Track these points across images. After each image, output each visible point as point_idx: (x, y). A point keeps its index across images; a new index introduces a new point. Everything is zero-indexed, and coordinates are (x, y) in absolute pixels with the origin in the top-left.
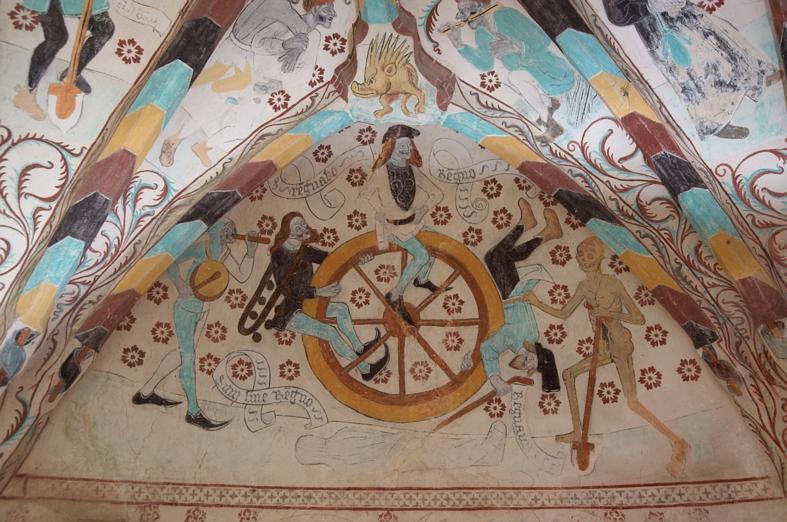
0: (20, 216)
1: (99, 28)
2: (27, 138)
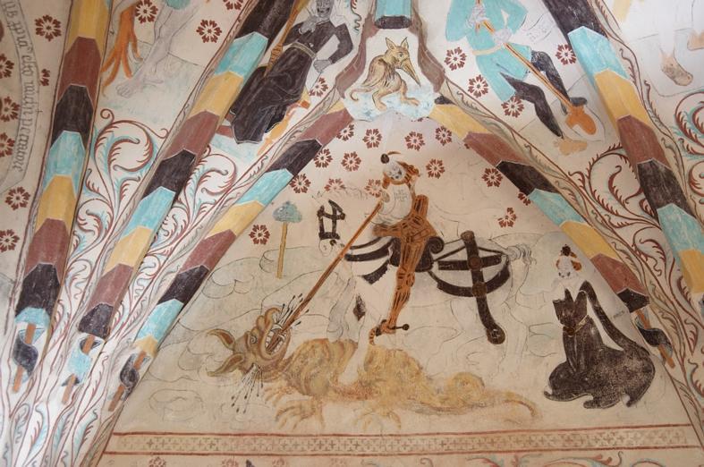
0: (636, 217)
1: (541, 63)
2: (591, 167)
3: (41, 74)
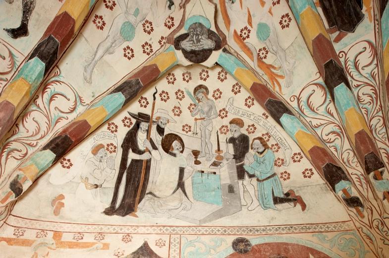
3: (264, 116)
